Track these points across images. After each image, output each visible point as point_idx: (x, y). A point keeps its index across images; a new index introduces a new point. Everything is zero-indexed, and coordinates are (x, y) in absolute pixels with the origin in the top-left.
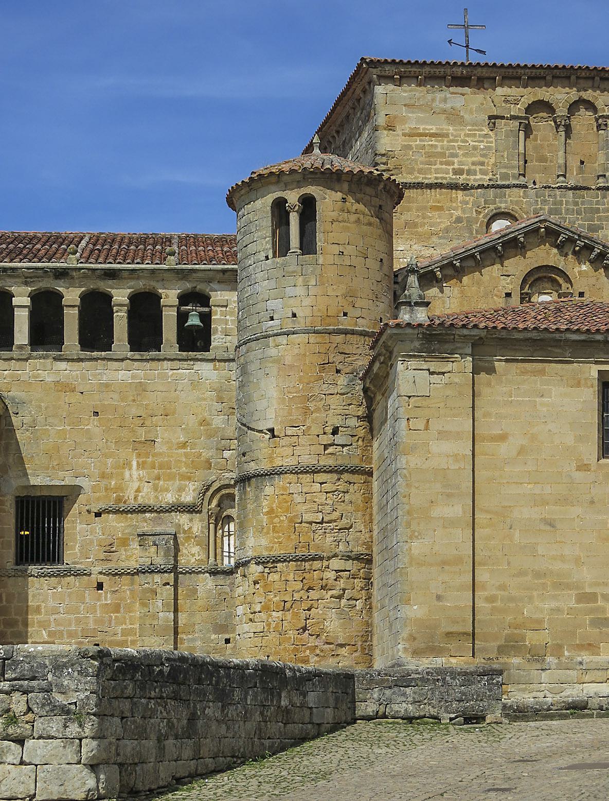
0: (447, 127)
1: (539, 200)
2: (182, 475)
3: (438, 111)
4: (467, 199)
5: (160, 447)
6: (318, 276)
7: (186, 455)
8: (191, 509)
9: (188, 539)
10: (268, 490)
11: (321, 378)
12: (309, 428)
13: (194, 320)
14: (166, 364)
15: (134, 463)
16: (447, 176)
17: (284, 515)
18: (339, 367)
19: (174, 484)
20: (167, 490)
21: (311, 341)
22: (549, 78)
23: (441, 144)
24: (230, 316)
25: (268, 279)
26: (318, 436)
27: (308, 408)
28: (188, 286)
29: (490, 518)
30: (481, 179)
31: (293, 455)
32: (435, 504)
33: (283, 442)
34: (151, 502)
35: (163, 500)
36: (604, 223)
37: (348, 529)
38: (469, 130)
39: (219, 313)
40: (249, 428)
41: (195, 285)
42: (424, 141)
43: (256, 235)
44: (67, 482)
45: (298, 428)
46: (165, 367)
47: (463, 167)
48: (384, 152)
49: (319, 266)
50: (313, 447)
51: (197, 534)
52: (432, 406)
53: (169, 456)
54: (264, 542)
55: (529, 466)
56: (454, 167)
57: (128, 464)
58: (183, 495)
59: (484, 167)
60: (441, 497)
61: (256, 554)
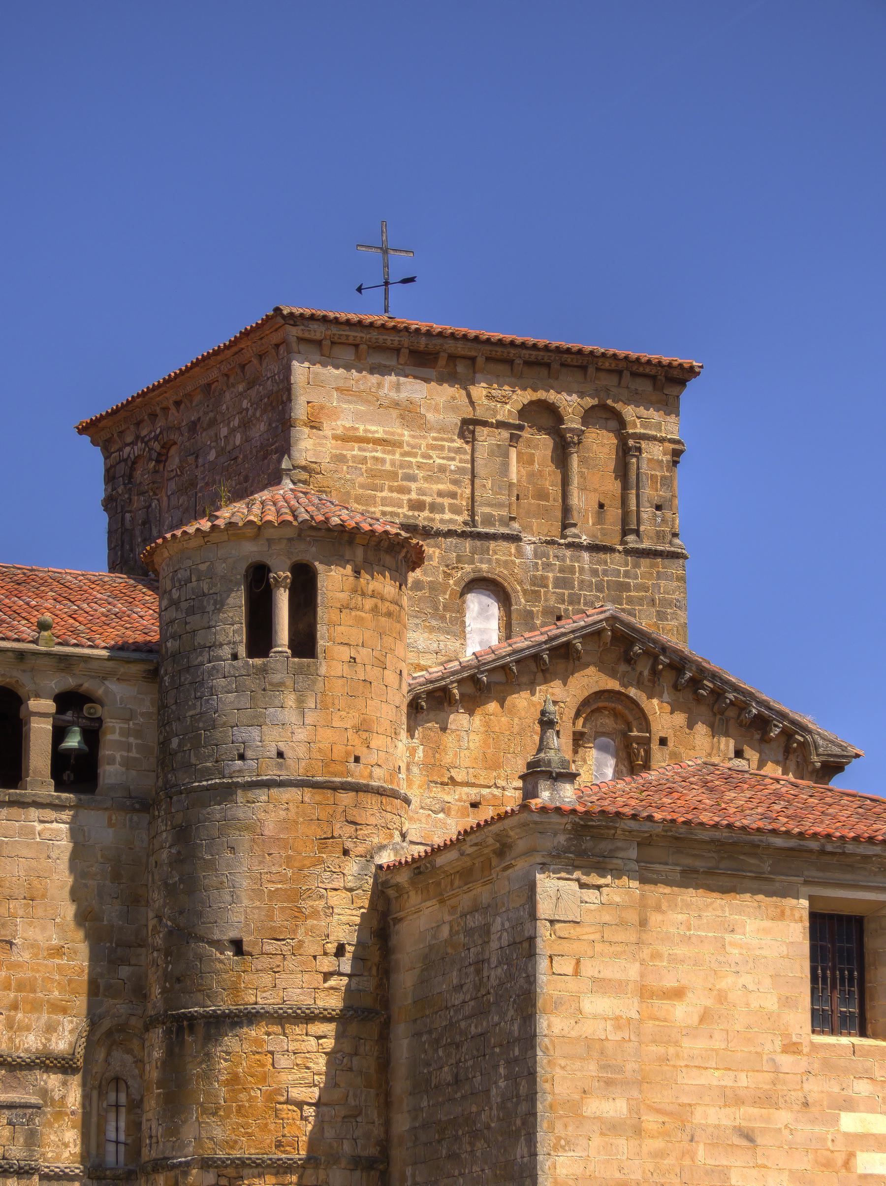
0: (399, 431)
1: (540, 562)
2: (52, 1004)
3: (386, 402)
4: (431, 552)
6: (319, 695)
7: (60, 968)
9: (59, 1115)
12: (301, 942)
14: (34, 813)
16: (400, 511)
17: (258, 1089)
18: (349, 845)
19: (38, 1018)
20: (28, 1029)
21: (306, 799)
22: (555, 366)
23: (391, 457)
24: (136, 738)
25: (236, 692)
26: (315, 957)
29: (664, 1123)
30: (451, 521)
31: (275, 987)
32: (588, 1096)
35: (22, 1045)
36: (637, 608)
37: (355, 1117)
38: (435, 439)
39: (118, 731)
41: (80, 682)
42: (365, 450)
45: (284, 942)
46: (32, 818)
47: (424, 498)
48: (303, 463)
49: (319, 678)
50: (306, 976)
51: (73, 1108)
52: (585, 937)
53: (33, 970)
55: (716, 1041)
56: (411, 497)
58: (54, 1040)
59: (455, 501)
60: (597, 1084)
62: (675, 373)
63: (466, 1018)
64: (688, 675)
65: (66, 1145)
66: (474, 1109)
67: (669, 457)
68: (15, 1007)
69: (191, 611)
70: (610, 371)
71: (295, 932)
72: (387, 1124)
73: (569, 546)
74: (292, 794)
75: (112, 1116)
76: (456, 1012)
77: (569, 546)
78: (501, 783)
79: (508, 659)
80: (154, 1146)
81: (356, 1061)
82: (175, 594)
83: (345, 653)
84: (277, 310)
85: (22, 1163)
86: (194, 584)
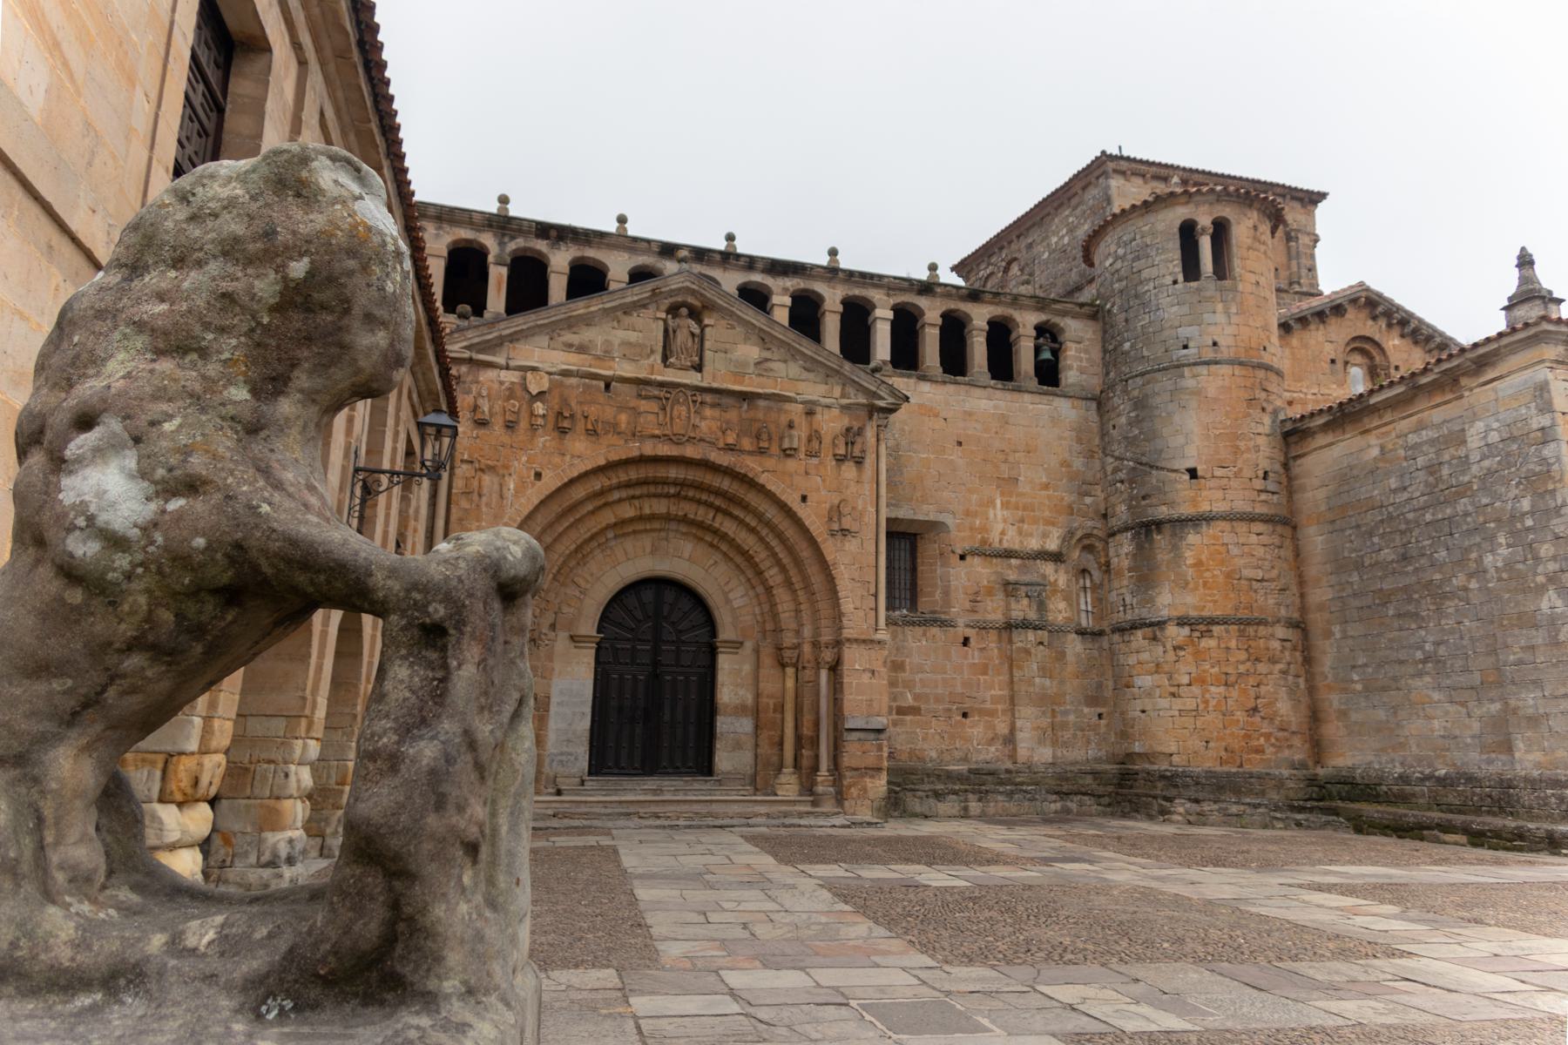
5: (1024, 487)
7: (1049, 497)
8: (1057, 557)
9: (1055, 592)
10: (1192, 538)
11: (1249, 415)
12: (1241, 470)
13: (1047, 355)
15: (998, 502)
18: (1265, 405)
20: (1031, 535)
21: (1237, 373)
27: (1237, 447)
28: (1043, 317)
33: (1212, 483)
34: (1017, 547)
40: (1152, 467)
43: (1158, 259)
44: (932, 517)
50: (1246, 493)
54: (1190, 599)
57: (991, 503)
61: (1175, 614)
62: (1314, 197)
63: (1415, 510)
64: (1413, 326)
65: (1060, 612)
66: (1438, 576)
68: (1022, 521)
69: (1138, 258)
71: (1235, 462)
72: (1302, 596)
74: (1225, 370)
75: (1082, 595)
76: (1396, 509)
78: (1305, 390)
80: (1129, 612)
81: (1282, 553)
82: (1121, 252)
83: (1253, 278)
84: (1103, 153)
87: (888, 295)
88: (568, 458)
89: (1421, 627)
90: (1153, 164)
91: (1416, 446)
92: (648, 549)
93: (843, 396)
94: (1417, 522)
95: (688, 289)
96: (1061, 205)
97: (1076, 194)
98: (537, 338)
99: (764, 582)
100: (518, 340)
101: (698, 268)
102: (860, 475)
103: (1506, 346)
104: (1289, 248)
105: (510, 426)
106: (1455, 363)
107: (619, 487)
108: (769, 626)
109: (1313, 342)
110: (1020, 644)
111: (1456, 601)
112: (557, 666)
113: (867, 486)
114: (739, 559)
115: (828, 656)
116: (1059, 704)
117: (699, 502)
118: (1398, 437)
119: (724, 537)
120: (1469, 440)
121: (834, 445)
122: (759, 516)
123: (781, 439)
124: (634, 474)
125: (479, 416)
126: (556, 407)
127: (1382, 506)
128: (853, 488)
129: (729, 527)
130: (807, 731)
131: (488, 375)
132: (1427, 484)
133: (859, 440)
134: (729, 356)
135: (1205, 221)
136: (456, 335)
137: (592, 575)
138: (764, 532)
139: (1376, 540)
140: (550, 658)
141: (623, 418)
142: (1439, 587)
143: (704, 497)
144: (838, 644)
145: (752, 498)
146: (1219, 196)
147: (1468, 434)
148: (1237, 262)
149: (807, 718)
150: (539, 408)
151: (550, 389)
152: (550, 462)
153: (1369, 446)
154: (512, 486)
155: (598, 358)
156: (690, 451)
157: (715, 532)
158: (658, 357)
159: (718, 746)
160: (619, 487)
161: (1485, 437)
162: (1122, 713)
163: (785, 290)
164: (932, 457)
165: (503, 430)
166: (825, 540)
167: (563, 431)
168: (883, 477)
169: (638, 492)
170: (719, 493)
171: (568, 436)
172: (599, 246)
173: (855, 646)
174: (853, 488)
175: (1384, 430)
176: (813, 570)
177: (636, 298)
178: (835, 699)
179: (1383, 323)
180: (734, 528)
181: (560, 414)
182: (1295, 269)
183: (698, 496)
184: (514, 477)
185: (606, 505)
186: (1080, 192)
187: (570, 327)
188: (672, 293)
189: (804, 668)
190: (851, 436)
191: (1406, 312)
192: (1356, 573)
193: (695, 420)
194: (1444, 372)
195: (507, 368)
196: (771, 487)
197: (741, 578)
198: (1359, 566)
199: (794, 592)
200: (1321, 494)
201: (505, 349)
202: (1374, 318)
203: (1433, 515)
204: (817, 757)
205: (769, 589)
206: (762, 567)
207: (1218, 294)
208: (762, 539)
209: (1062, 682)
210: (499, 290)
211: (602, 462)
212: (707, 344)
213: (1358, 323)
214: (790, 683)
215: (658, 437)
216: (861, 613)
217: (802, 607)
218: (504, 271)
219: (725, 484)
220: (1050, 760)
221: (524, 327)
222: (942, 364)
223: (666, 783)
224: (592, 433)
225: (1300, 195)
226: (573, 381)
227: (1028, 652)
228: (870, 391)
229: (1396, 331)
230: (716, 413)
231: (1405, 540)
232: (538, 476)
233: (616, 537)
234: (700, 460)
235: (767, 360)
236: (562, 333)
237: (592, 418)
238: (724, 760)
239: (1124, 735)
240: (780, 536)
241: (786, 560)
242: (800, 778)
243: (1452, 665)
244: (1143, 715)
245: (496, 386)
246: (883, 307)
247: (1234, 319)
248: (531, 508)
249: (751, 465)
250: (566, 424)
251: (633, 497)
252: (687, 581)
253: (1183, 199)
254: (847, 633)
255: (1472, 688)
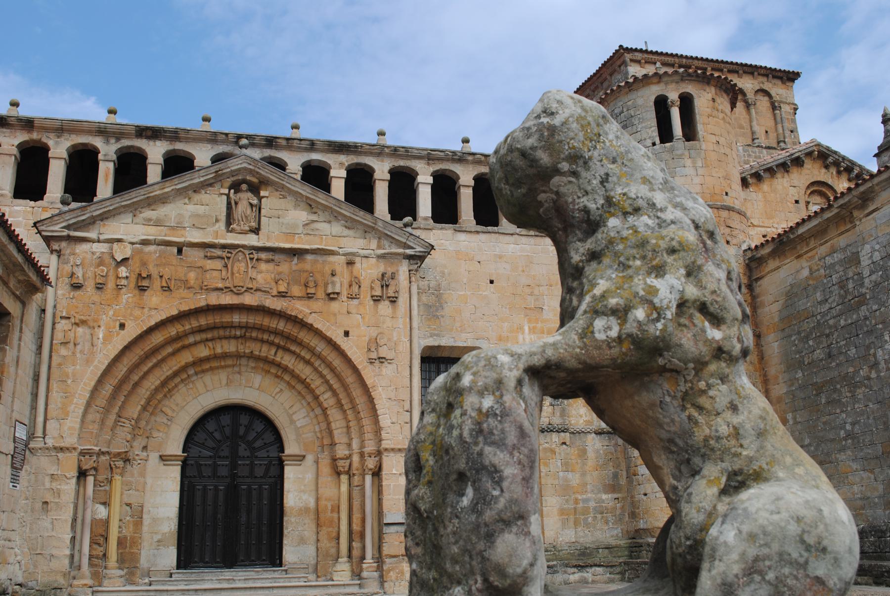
15: (526, 328)
18: (729, 239)
43: (640, 126)
57: (520, 329)
62: (791, 76)
63: (834, 317)
64: (856, 172)
65: (581, 416)
66: (851, 370)
67: (792, 111)
70: (763, 75)
73: (758, 146)
76: (822, 317)
77: (758, 146)
78: (776, 226)
79: (772, 164)
83: (713, 139)
84: (621, 46)
85: (560, 427)
86: (625, 113)
87: (428, 164)
88: (146, 310)
89: (842, 411)
90: (662, 54)
91: (832, 265)
92: (224, 382)
93: (379, 247)
94: (836, 327)
95: (245, 169)
96: (597, 88)
97: (605, 79)
98: (122, 216)
99: (320, 405)
100: (107, 218)
101: (268, 152)
102: (394, 312)
103: (877, 184)
104: (775, 115)
105: (100, 287)
106: (846, 199)
107: (193, 332)
108: (326, 441)
109: (780, 187)
110: (547, 445)
111: (863, 389)
112: (149, 481)
113: (401, 321)
114: (299, 387)
115: (371, 463)
116: (582, 493)
117: (262, 341)
118: (820, 260)
119: (286, 369)
120: (862, 259)
121: (372, 288)
122: (312, 351)
123: (326, 285)
124: (203, 321)
125: (75, 281)
126: (137, 271)
127: (813, 316)
128: (389, 323)
129: (288, 360)
130: (356, 527)
131: (85, 247)
132: (840, 296)
133: (392, 282)
134: (281, 220)
135: (673, 96)
136: (56, 218)
137: (177, 405)
138: (317, 363)
139: (811, 343)
140: (143, 474)
141: (192, 275)
142: (853, 378)
143: (266, 337)
144: (379, 453)
145: (304, 336)
146: (683, 76)
147: (861, 254)
148: (700, 128)
149: (356, 516)
150: (123, 271)
151: (133, 256)
152: (131, 315)
153: (802, 268)
154: (101, 336)
155: (172, 228)
156: (248, 300)
157: (279, 365)
158: (222, 225)
159: (285, 542)
160: (193, 332)
161: (871, 257)
162: (632, 497)
163: (341, 164)
164: (469, 293)
165: (94, 291)
166: (365, 368)
167: (142, 289)
168: (415, 312)
169: (209, 335)
170: (276, 333)
171: (146, 293)
172: (187, 140)
173: (392, 454)
174: (389, 323)
175: (809, 254)
176: (357, 392)
177: (202, 179)
178: (379, 499)
179: (833, 170)
180: (293, 361)
181: (140, 275)
182: (780, 131)
183: (260, 336)
184: (102, 328)
185: (184, 347)
186: (608, 77)
187: (149, 205)
188: (233, 173)
189: (354, 475)
190: (385, 281)
191: (850, 161)
192: (800, 371)
193: (252, 273)
194: (841, 206)
195: (99, 241)
196: (318, 325)
197: (303, 402)
198: (800, 364)
199: (344, 411)
200: (776, 307)
201: (96, 226)
202: (827, 167)
203: (845, 320)
204: (364, 548)
205: (324, 410)
206: (318, 392)
207: (686, 153)
208: (316, 369)
209: (583, 474)
210: (106, 180)
211: (175, 312)
212: (263, 211)
213: (813, 172)
214: (344, 488)
215: (222, 289)
216: (398, 427)
217: (351, 424)
218: (111, 166)
219: (281, 325)
220: (574, 540)
221: (111, 208)
222: (476, 217)
223: (240, 574)
224: (167, 289)
225: (779, 74)
226: (152, 248)
227: (553, 452)
228: (401, 242)
229: (844, 177)
230: (270, 266)
231: (829, 342)
232: (122, 326)
233: (196, 373)
234: (257, 306)
235: (313, 221)
236: (143, 210)
237: (166, 277)
238: (290, 554)
239: (633, 515)
240: (329, 366)
241: (336, 386)
242: (352, 566)
243: (864, 440)
244: (644, 498)
245: (89, 256)
246: (424, 174)
247: (700, 171)
248: (116, 352)
249: (300, 308)
250: (145, 283)
251: (207, 340)
252: (258, 407)
253: (655, 80)
254: (385, 444)
255: (877, 458)
